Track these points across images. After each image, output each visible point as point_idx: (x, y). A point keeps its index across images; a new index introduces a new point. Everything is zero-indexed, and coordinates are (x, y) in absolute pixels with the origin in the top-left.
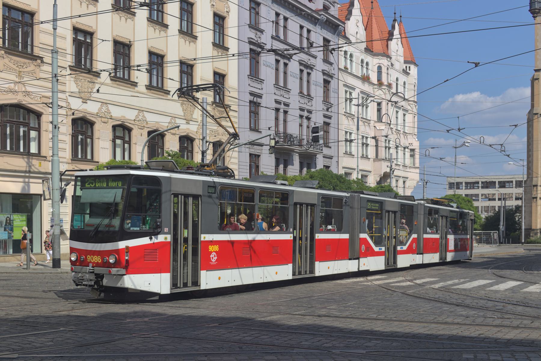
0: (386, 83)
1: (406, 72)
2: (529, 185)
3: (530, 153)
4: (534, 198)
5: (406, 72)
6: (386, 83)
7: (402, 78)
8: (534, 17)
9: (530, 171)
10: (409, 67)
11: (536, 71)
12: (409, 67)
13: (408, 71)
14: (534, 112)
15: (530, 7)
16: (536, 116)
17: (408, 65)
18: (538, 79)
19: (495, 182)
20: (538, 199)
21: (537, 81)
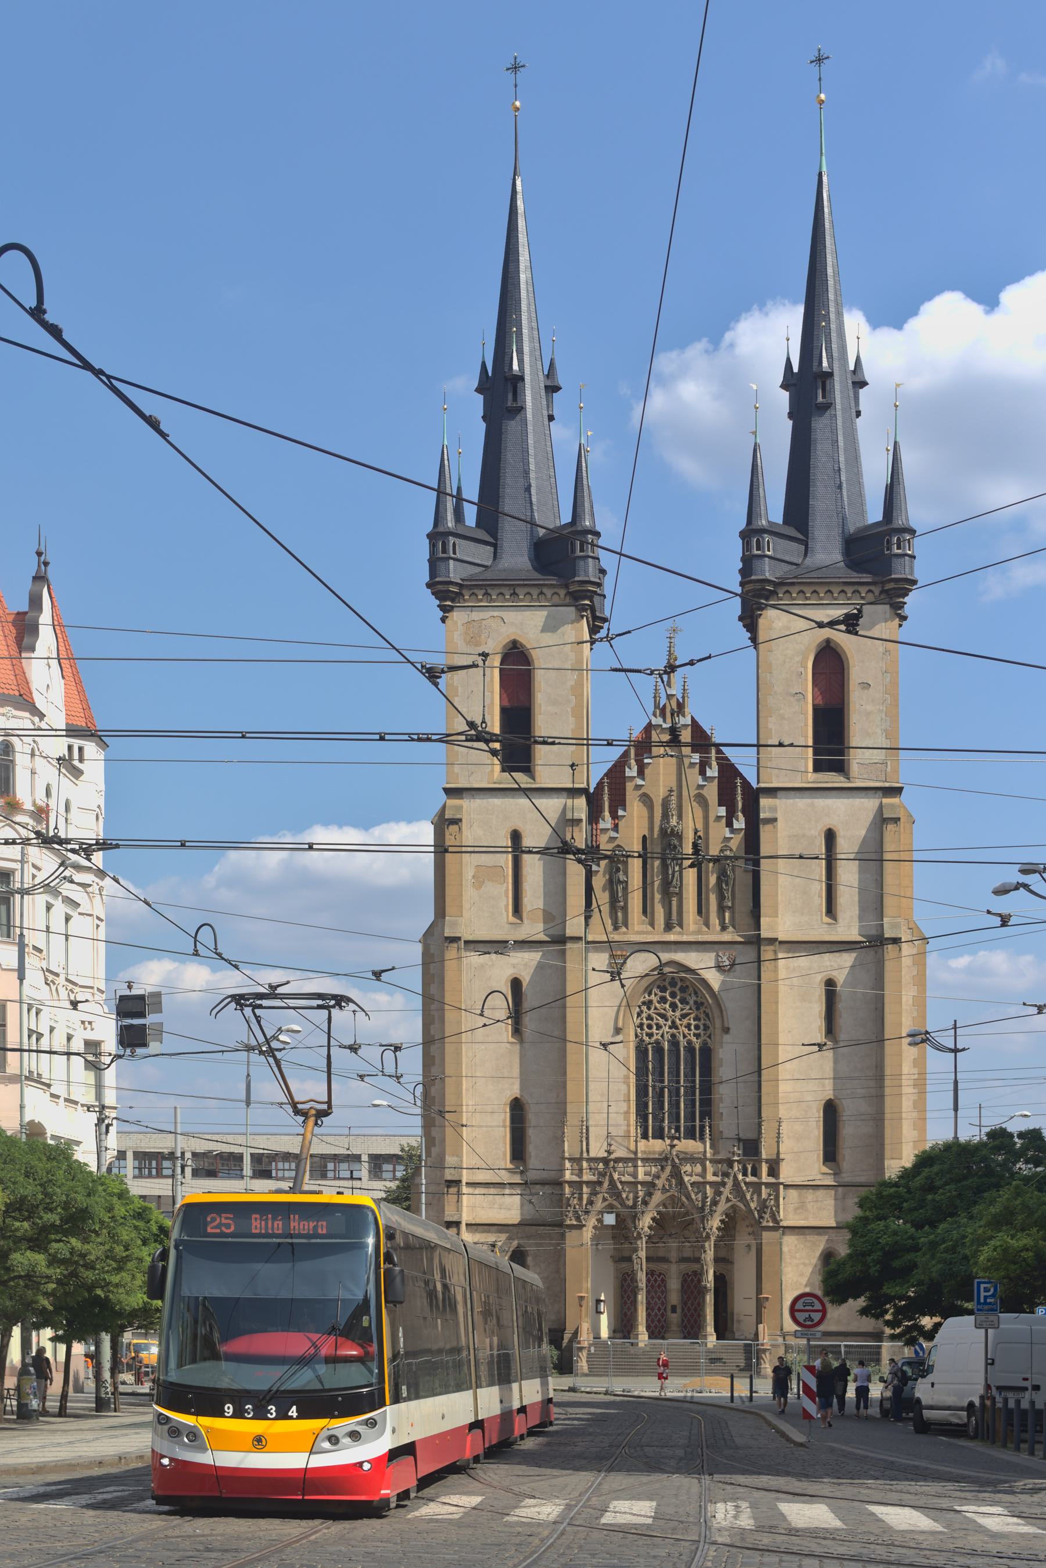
0: (28, 806)
1: (69, 765)
2: (419, 1176)
3: (434, 1071)
4: (449, 1225)
5: (69, 765)
6: (28, 806)
7: (66, 788)
8: (444, 609)
9: (435, 1132)
10: (81, 749)
11: (449, 792)
12: (81, 749)
13: (76, 763)
14: (448, 933)
15: (433, 572)
16: (455, 945)
17: (76, 743)
18: (457, 822)
19: (239, 1158)
20: (463, 1227)
21: (453, 828)
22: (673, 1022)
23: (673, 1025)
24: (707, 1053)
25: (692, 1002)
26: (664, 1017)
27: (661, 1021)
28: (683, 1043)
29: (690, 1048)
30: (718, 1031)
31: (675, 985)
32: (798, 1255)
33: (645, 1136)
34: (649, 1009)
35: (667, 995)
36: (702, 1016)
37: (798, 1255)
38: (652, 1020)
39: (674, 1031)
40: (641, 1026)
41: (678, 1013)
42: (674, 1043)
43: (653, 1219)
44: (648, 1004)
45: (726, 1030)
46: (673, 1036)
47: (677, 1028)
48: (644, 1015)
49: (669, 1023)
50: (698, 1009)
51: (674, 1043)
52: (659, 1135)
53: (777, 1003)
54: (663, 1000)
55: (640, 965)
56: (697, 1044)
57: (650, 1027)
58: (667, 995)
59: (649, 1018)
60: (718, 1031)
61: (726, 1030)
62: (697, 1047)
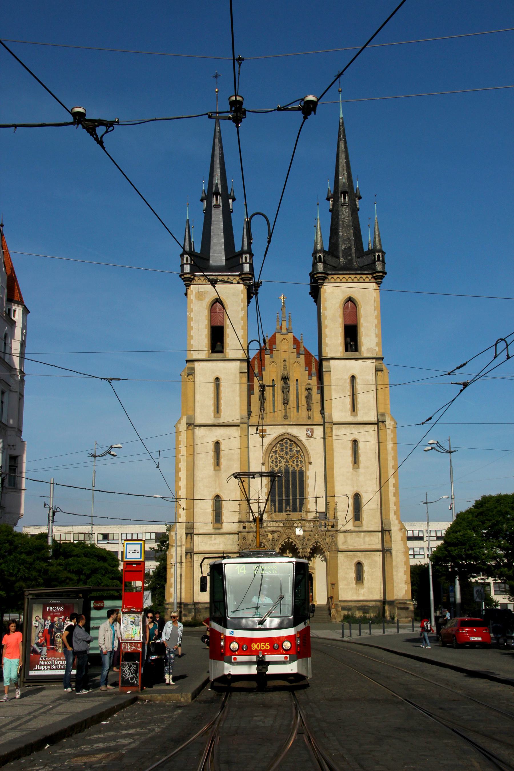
22: (287, 460)
23: (287, 462)
24: (302, 473)
25: (295, 451)
26: (282, 457)
27: (281, 460)
28: (291, 469)
29: (294, 472)
30: (307, 464)
31: (287, 442)
32: (344, 564)
33: (275, 512)
34: (276, 454)
35: (284, 448)
36: (300, 457)
37: (344, 564)
38: (277, 459)
39: (287, 464)
40: (272, 462)
41: (288, 456)
42: (287, 470)
43: (280, 549)
44: (275, 452)
45: (310, 463)
46: (287, 466)
47: (288, 462)
48: (274, 457)
49: (285, 460)
50: (297, 454)
51: (287, 470)
52: (280, 510)
53: (333, 450)
54: (282, 450)
55: (272, 433)
56: (297, 469)
57: (276, 462)
58: (284, 448)
59: (276, 458)
60: (307, 464)
61: (310, 463)
62: (297, 471)
